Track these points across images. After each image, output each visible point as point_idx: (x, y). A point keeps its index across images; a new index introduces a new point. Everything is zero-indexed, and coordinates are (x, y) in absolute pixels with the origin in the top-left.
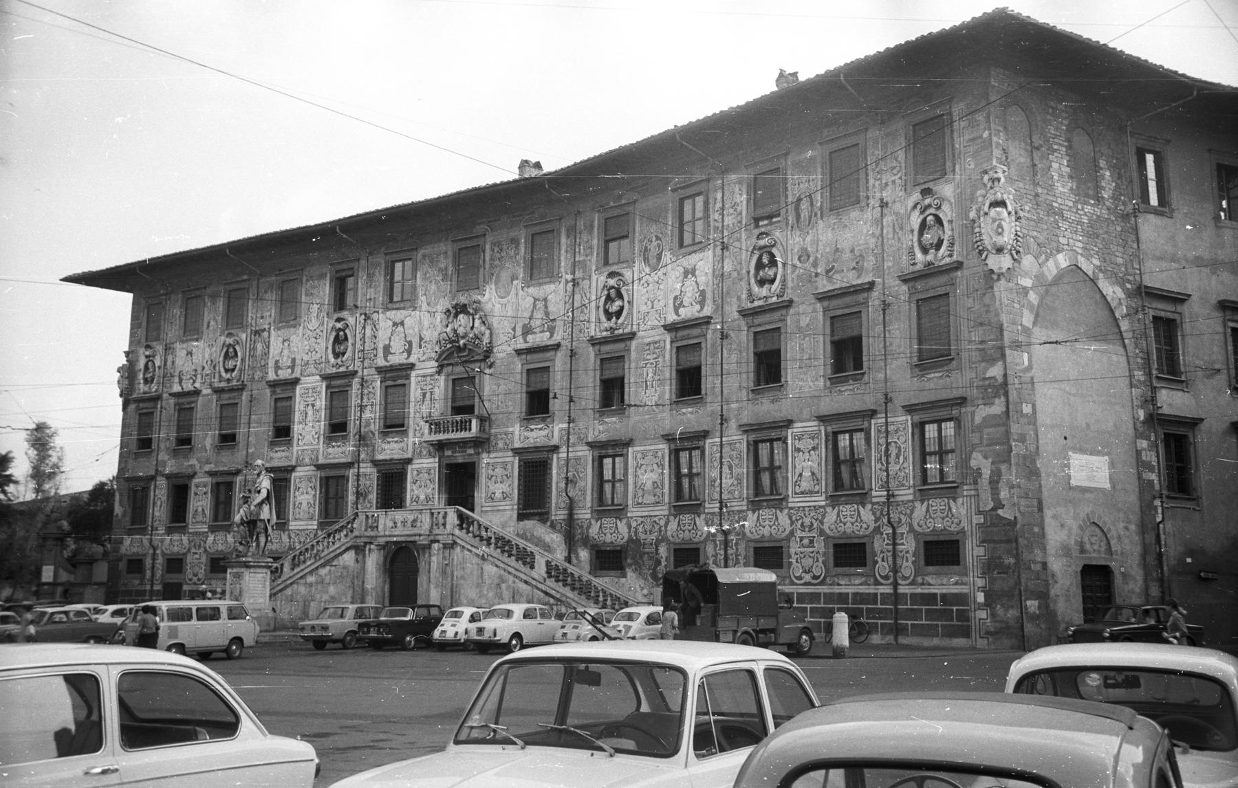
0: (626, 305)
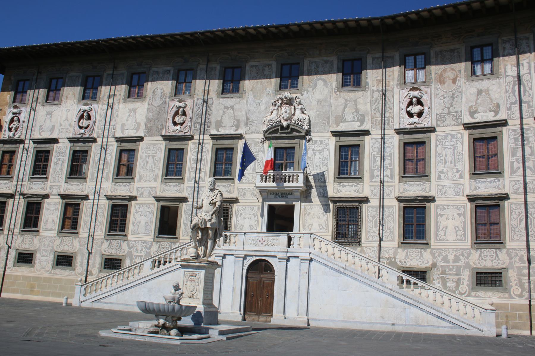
0: (426, 108)
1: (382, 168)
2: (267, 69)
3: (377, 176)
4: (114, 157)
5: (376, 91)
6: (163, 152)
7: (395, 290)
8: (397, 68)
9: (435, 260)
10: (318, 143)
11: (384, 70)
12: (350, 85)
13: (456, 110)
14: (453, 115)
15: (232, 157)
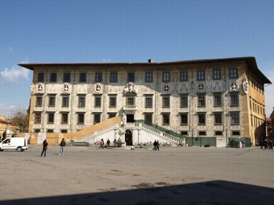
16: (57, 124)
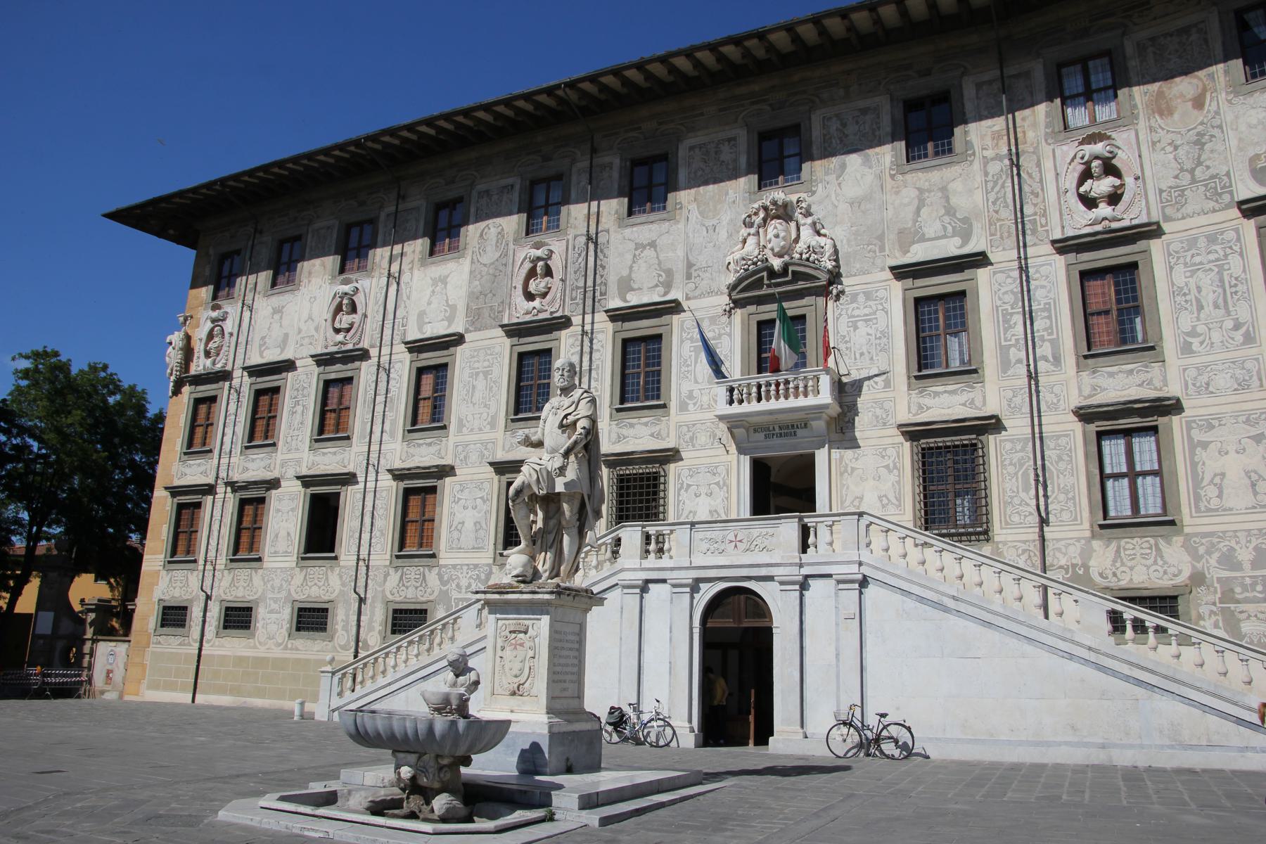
0: (1129, 180)
1: (1030, 341)
2: (725, 148)
3: (1019, 361)
4: (405, 385)
5: (992, 159)
6: (507, 361)
7: (1103, 649)
8: (1042, 109)
9: (1199, 566)
10: (861, 298)
11: (1010, 116)
12: (926, 156)
13: (1212, 171)
14: (1206, 186)
15: (659, 357)
16: (281, 576)
